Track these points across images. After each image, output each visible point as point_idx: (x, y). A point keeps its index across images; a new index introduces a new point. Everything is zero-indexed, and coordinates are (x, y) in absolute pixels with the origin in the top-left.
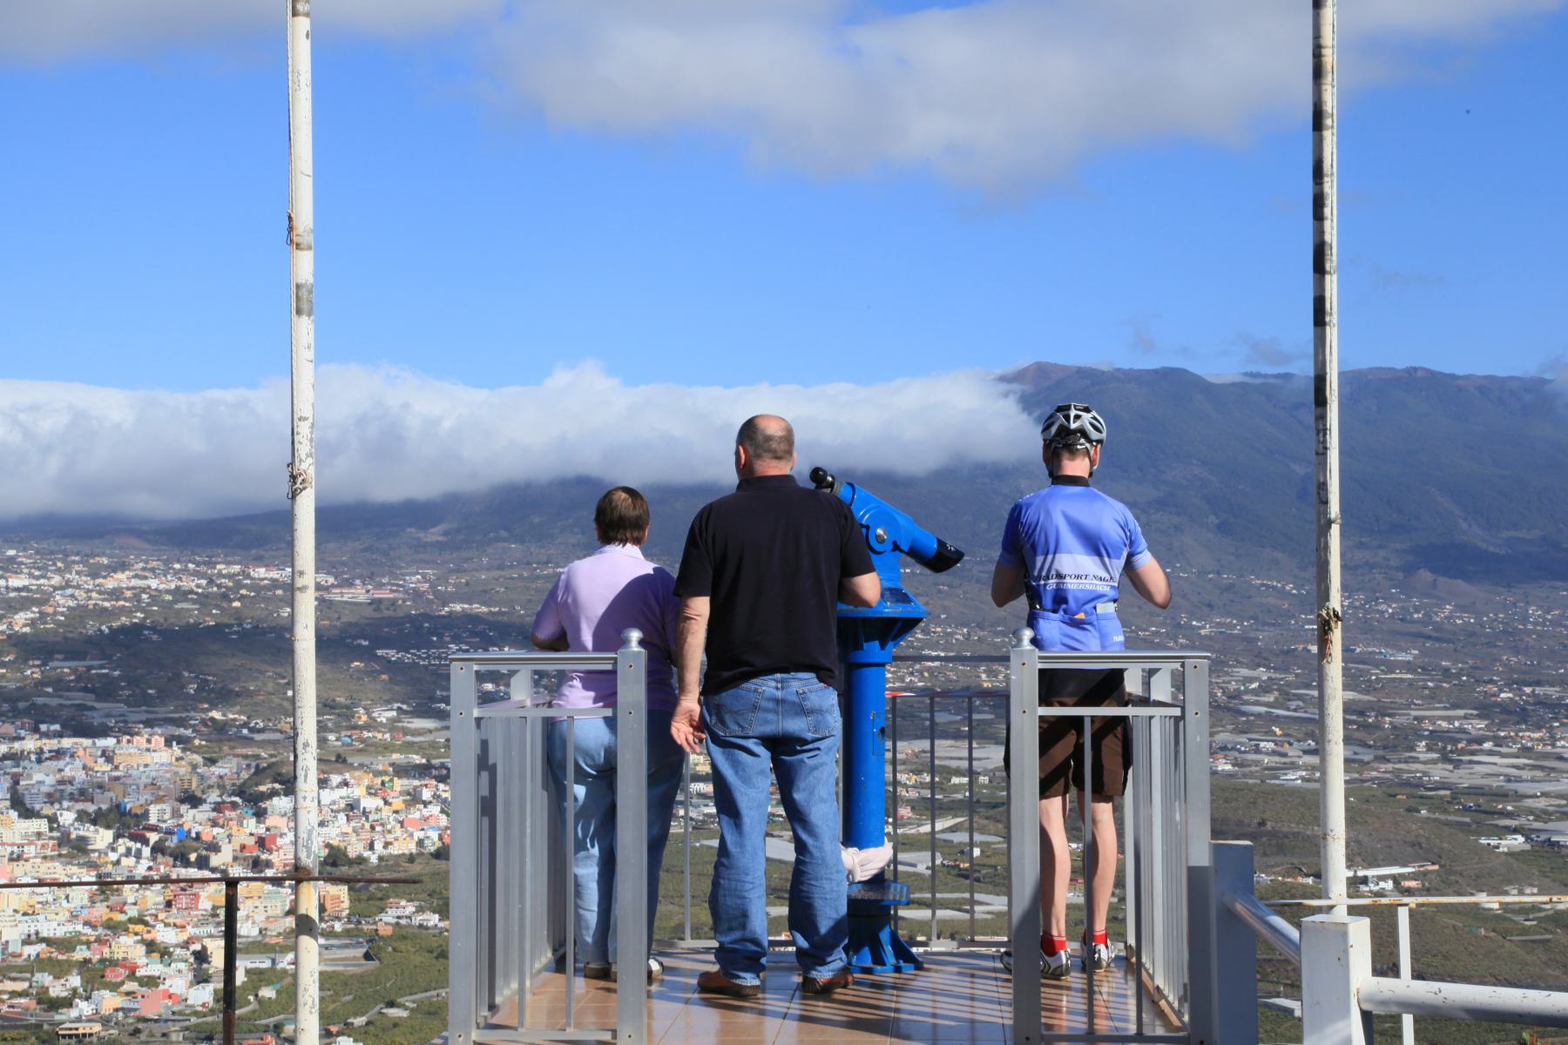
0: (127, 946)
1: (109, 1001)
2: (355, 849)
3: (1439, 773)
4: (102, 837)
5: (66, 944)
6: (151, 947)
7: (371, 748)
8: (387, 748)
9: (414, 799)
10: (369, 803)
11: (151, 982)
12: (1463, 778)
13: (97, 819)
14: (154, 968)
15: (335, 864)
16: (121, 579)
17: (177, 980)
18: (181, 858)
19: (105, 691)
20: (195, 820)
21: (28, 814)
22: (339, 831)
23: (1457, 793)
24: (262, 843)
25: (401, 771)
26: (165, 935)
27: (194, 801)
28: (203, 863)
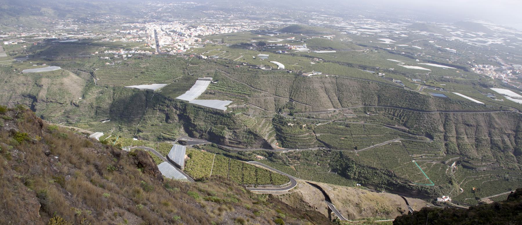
0: (176, 45)
1: (174, 51)
2: (202, 34)
3: (336, 25)
4: (172, 33)
5: (169, 45)
6: (179, 45)
7: (202, 22)
8: (205, 22)
9: (208, 28)
10: (203, 29)
11: (179, 49)
12: (339, 26)
13: (171, 31)
14: (179, 47)
15: (199, 36)
16: (171, 4)
17: (182, 49)
18: (181, 36)
19: (171, 17)
20: (183, 31)
21: (163, 31)
22: (199, 32)
23: (338, 27)
24: (191, 34)
25: (207, 25)
26: (180, 44)
27: (182, 29)
28: (184, 36)
